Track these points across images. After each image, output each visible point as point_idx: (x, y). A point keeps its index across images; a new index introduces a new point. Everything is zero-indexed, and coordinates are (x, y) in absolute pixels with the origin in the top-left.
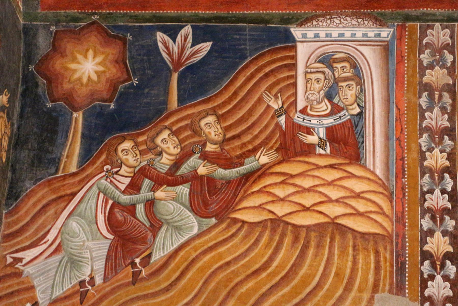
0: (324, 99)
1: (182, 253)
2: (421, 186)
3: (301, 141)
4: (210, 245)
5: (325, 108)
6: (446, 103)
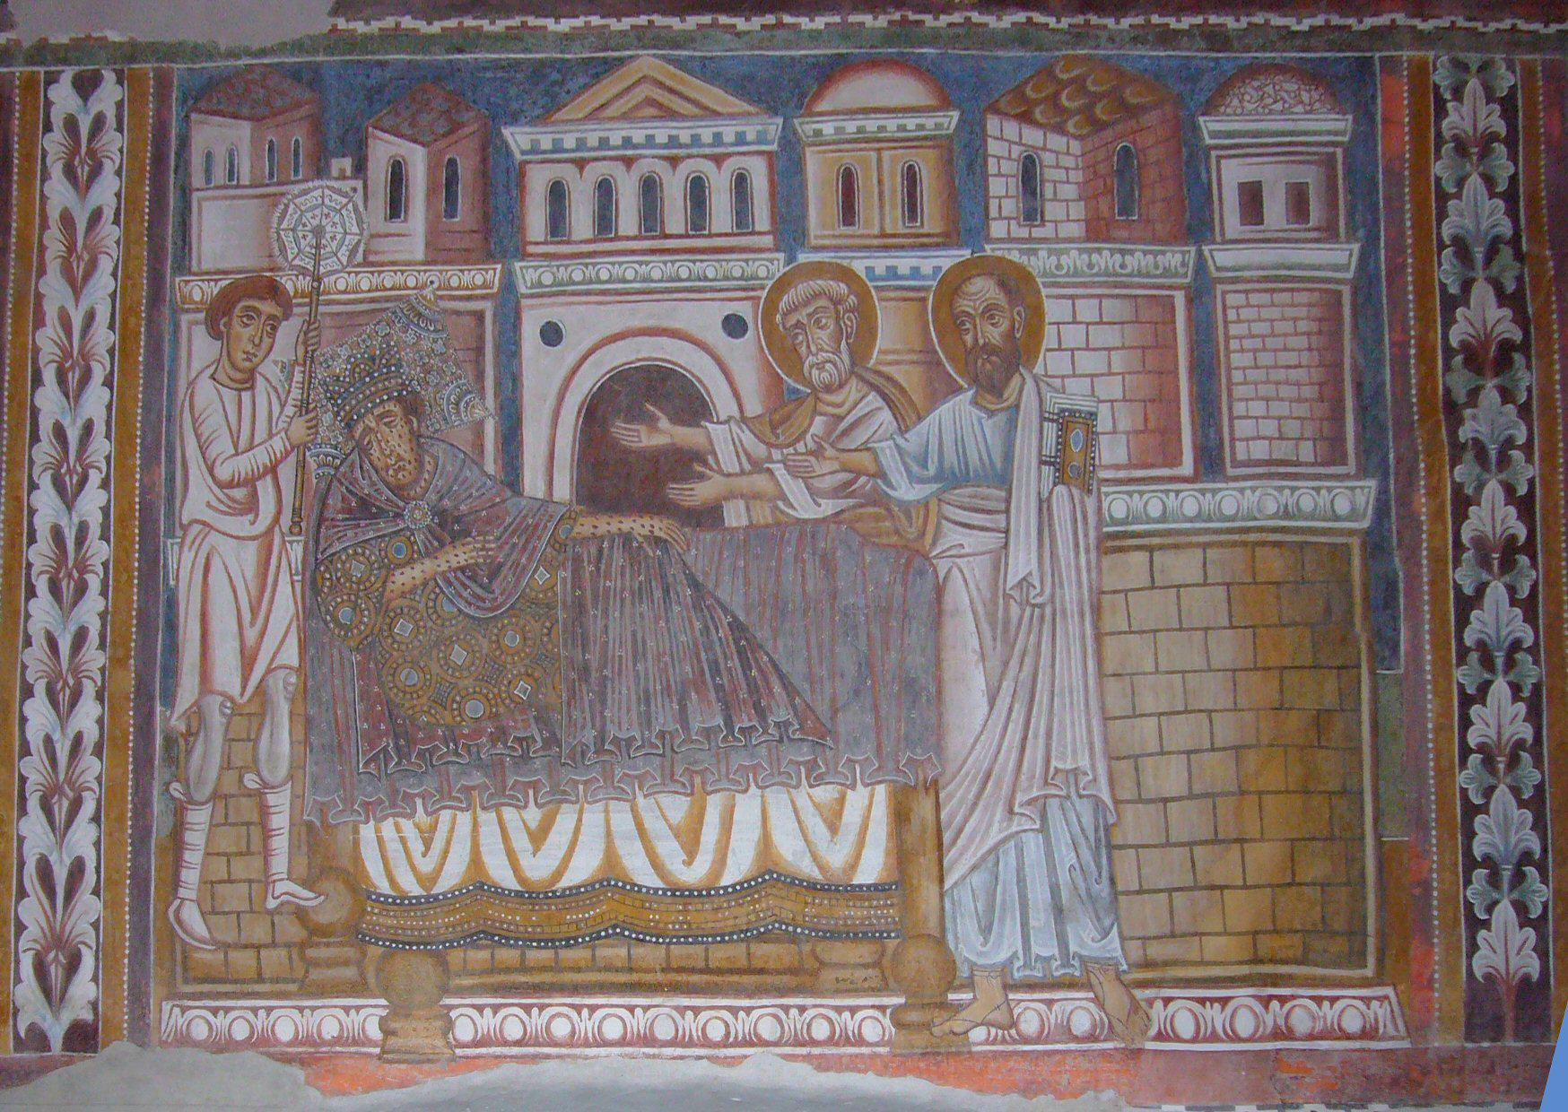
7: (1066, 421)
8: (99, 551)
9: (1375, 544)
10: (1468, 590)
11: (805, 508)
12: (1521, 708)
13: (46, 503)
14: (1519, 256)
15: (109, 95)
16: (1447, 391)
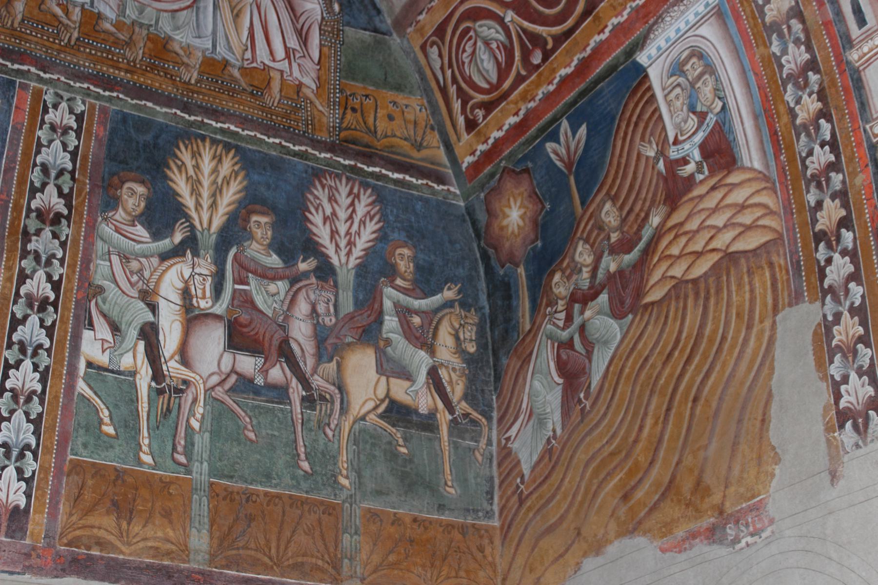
0: (688, 116)
1: (611, 369)
2: (800, 153)
3: (682, 177)
4: (631, 346)
5: (692, 123)
6: (797, 33)
10: (19, 316)
12: (37, 375)
14: (73, 178)
16: (25, 226)
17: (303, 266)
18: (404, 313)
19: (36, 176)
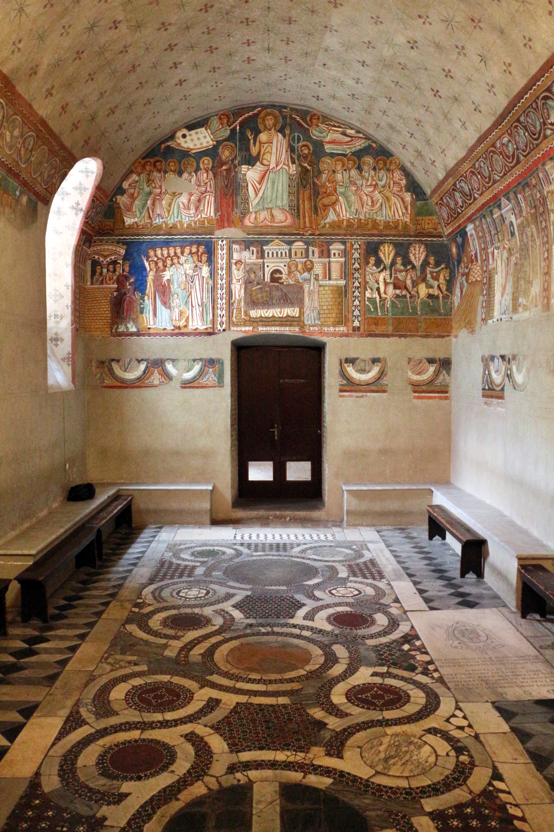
7: (316, 275)
8: (225, 286)
9: (345, 286)
11: (291, 283)
13: (220, 281)
15: (224, 242)
17: (409, 267)
18: (431, 273)
19: (353, 261)
